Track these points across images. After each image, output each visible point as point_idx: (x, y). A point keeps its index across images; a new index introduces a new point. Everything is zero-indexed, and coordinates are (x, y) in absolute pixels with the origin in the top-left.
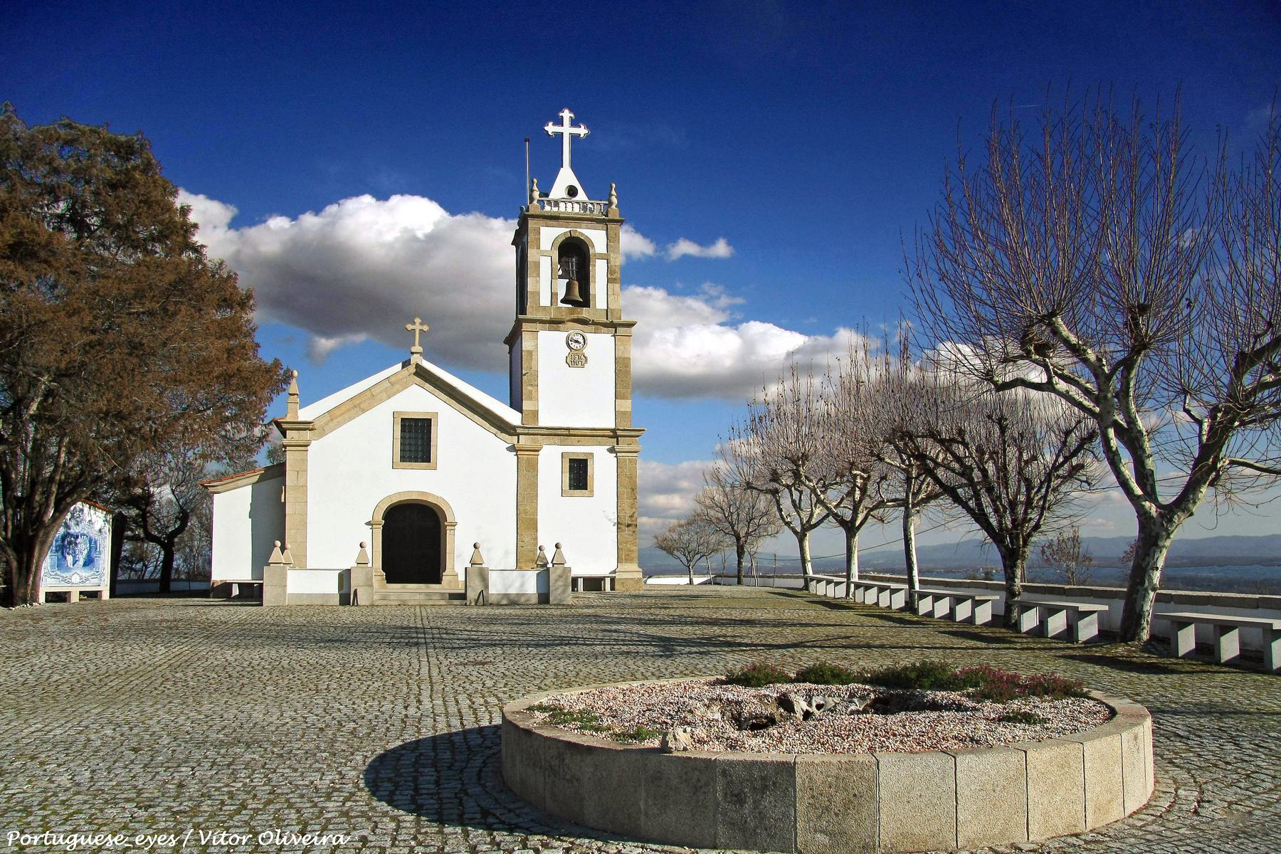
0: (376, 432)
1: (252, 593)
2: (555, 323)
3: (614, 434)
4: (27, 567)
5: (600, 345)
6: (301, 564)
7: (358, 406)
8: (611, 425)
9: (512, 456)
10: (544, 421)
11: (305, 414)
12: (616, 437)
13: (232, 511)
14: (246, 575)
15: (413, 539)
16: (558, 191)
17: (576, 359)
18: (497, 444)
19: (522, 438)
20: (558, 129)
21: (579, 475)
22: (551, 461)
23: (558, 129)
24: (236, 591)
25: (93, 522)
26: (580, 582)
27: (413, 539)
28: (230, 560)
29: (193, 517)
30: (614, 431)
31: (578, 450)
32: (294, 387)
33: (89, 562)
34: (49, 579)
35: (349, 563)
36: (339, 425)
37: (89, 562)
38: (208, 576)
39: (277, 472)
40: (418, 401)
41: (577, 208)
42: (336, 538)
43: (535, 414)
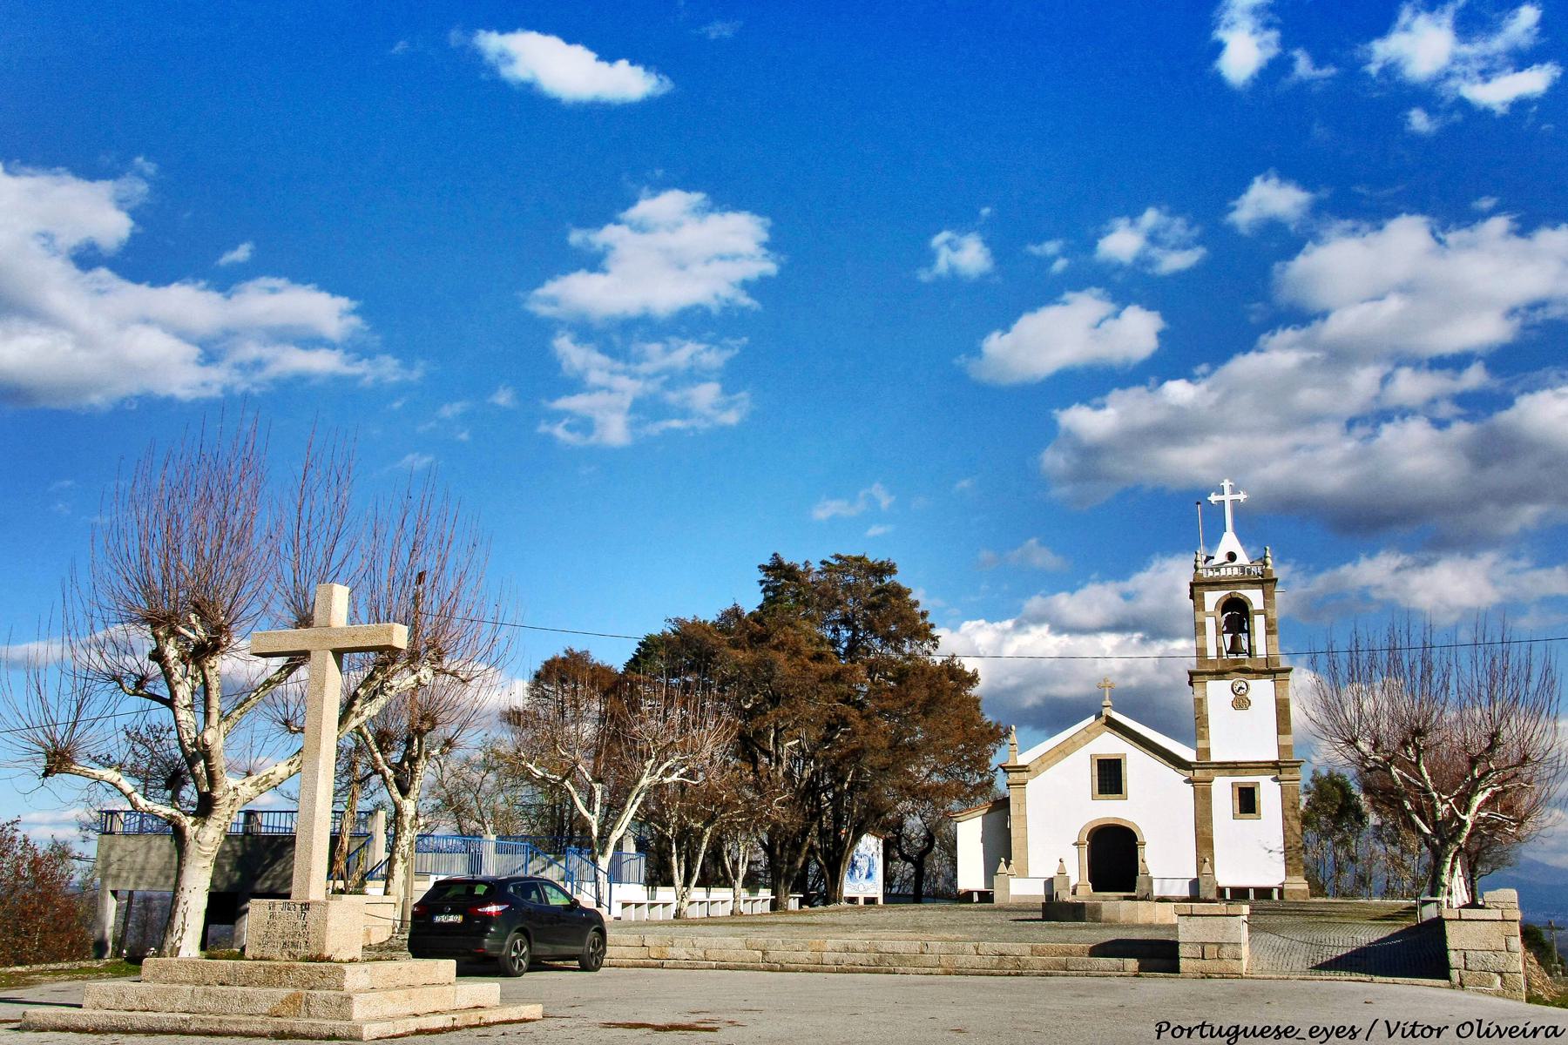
0: (1079, 771)
1: (986, 897)
2: (1220, 674)
3: (1276, 766)
4: (835, 880)
5: (1262, 691)
6: (1023, 873)
7: (1063, 751)
8: (1275, 758)
9: (1189, 788)
10: (1215, 758)
11: (1022, 760)
12: (1280, 768)
13: (970, 834)
14: (981, 886)
15: (1114, 856)
16: (1220, 556)
17: (1241, 702)
18: (1176, 777)
19: (1199, 772)
20: (1220, 498)
21: (1247, 801)
22: (1223, 790)
23: (1220, 498)
24: (976, 898)
25: (869, 847)
26: (1251, 892)
27: (1114, 856)
29: (941, 843)
30: (1275, 763)
31: (1246, 780)
32: (1013, 738)
33: (869, 875)
34: (848, 891)
35: (1052, 873)
36: (1049, 766)
37: (869, 875)
38: (955, 886)
39: (1002, 805)
40: (1110, 744)
41: (1236, 572)
43: (1207, 751)
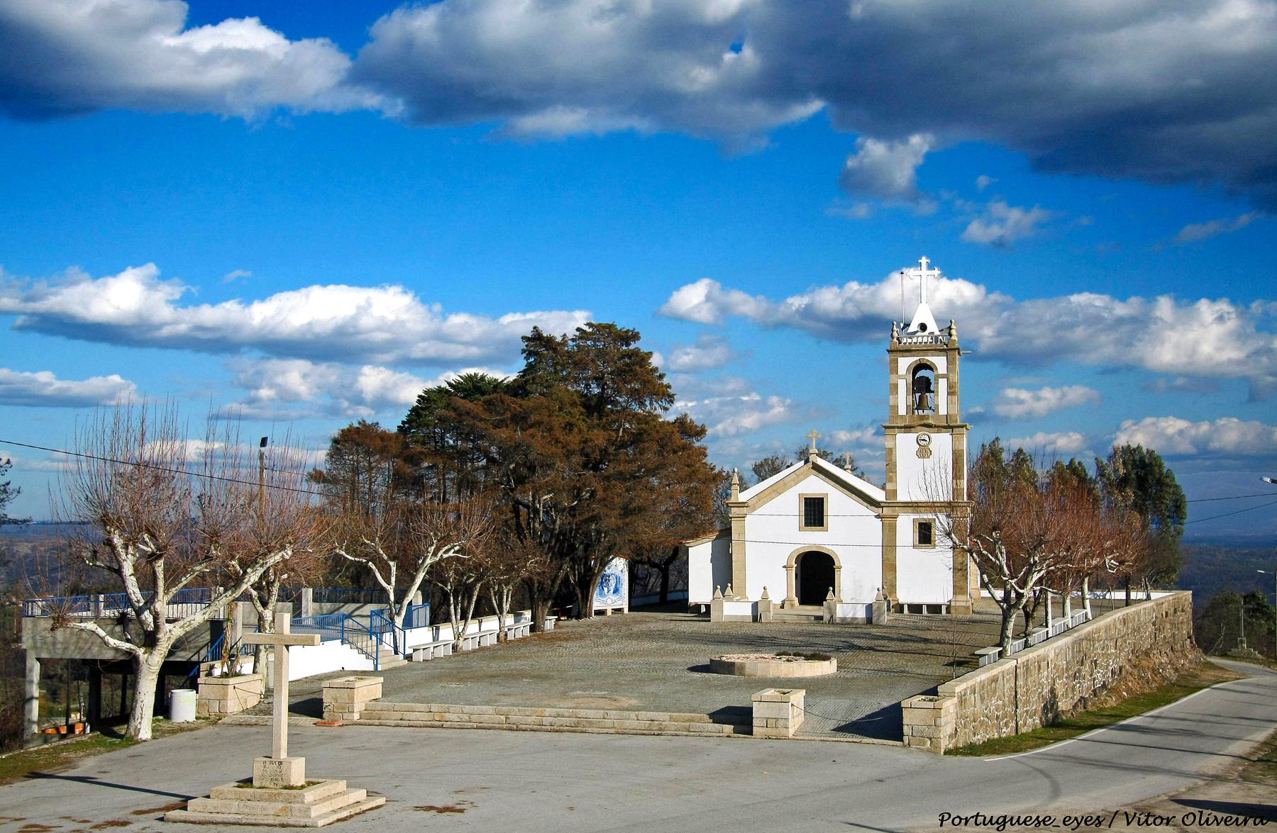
0: (790, 504)
2: (908, 428)
4: (586, 598)
7: (776, 490)
10: (902, 497)
13: (700, 556)
15: (815, 575)
17: (924, 452)
18: (870, 512)
19: (886, 510)
21: (925, 535)
22: (906, 526)
26: (925, 608)
27: (815, 575)
28: (700, 588)
29: (675, 562)
30: (950, 503)
33: (616, 591)
34: (597, 604)
36: (764, 503)
37: (616, 591)
39: (726, 533)
40: (815, 486)
42: (767, 577)
43: (895, 492)
